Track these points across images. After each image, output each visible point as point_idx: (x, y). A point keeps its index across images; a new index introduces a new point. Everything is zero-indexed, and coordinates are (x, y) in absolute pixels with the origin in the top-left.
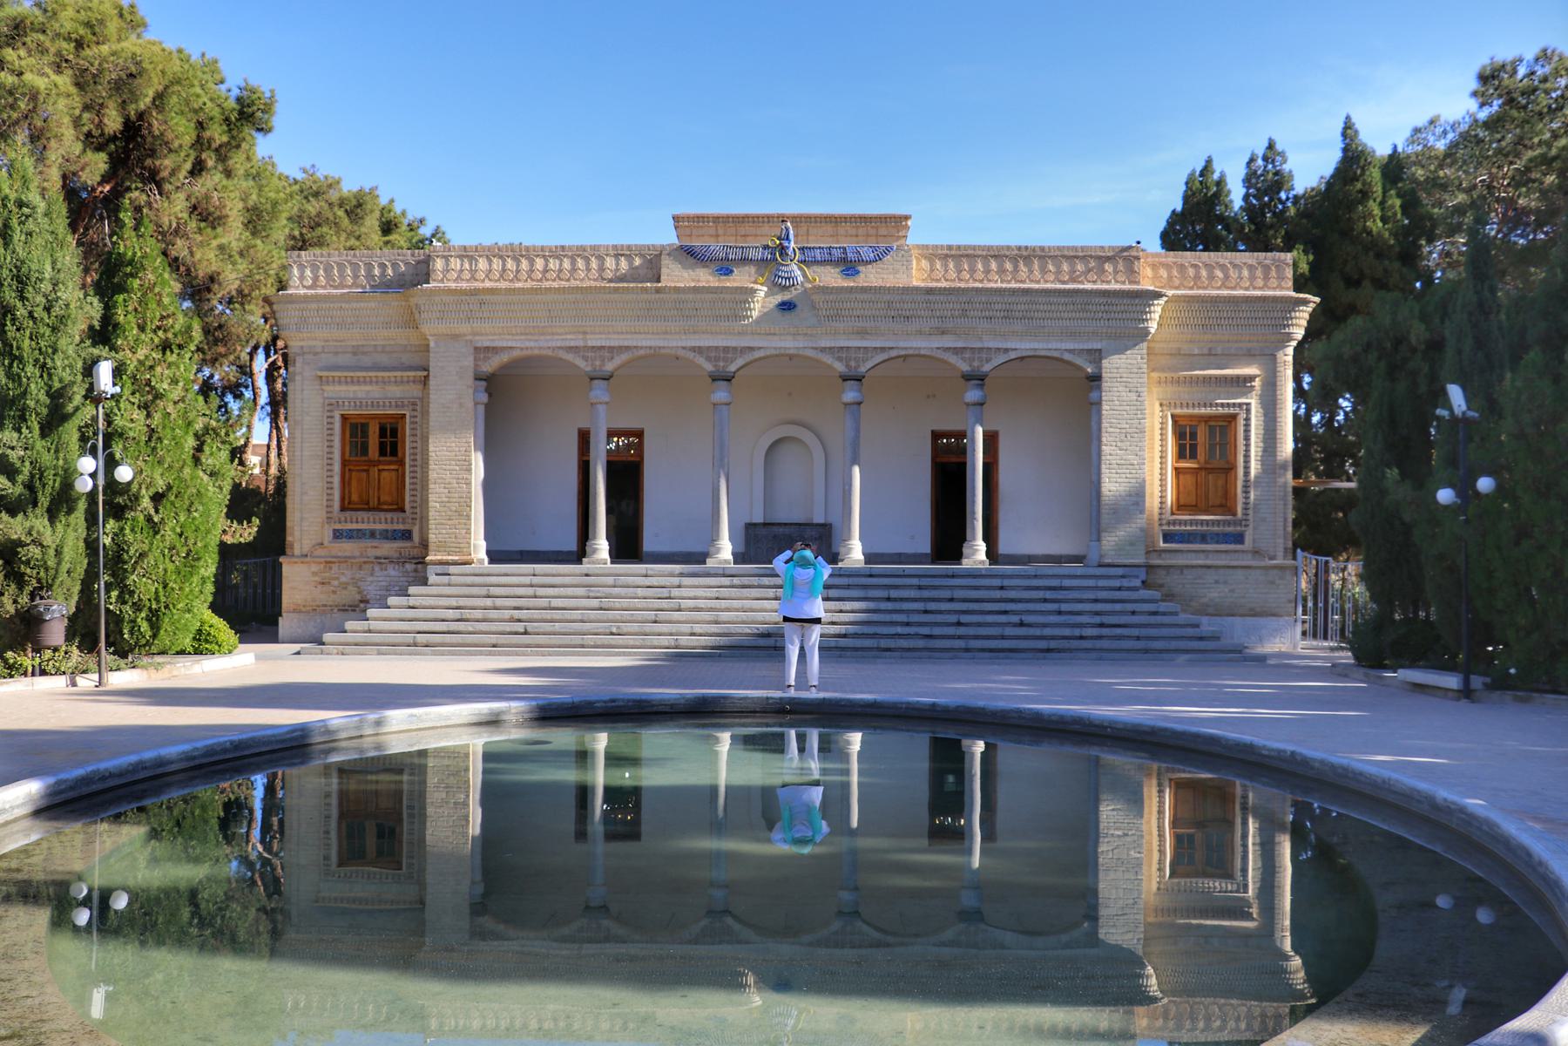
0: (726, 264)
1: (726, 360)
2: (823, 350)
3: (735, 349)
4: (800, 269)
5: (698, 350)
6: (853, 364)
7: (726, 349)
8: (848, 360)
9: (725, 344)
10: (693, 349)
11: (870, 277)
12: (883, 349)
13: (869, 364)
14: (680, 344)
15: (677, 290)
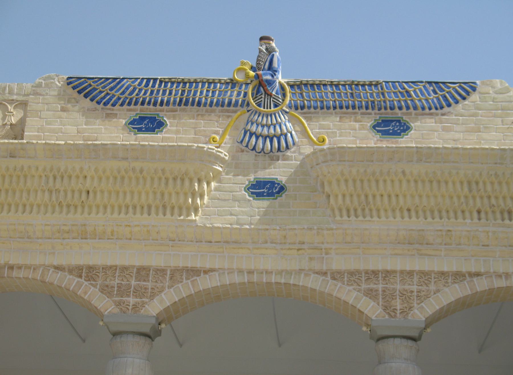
0: (149, 110)
1: (139, 292)
2: (336, 276)
3: (161, 271)
4: (293, 120)
5: (89, 273)
6: (398, 304)
7: (142, 272)
8: (388, 297)
9: (138, 262)
10: (78, 271)
11: (426, 132)
12: (459, 276)
13: (432, 306)
14: (50, 260)
15: (54, 151)
